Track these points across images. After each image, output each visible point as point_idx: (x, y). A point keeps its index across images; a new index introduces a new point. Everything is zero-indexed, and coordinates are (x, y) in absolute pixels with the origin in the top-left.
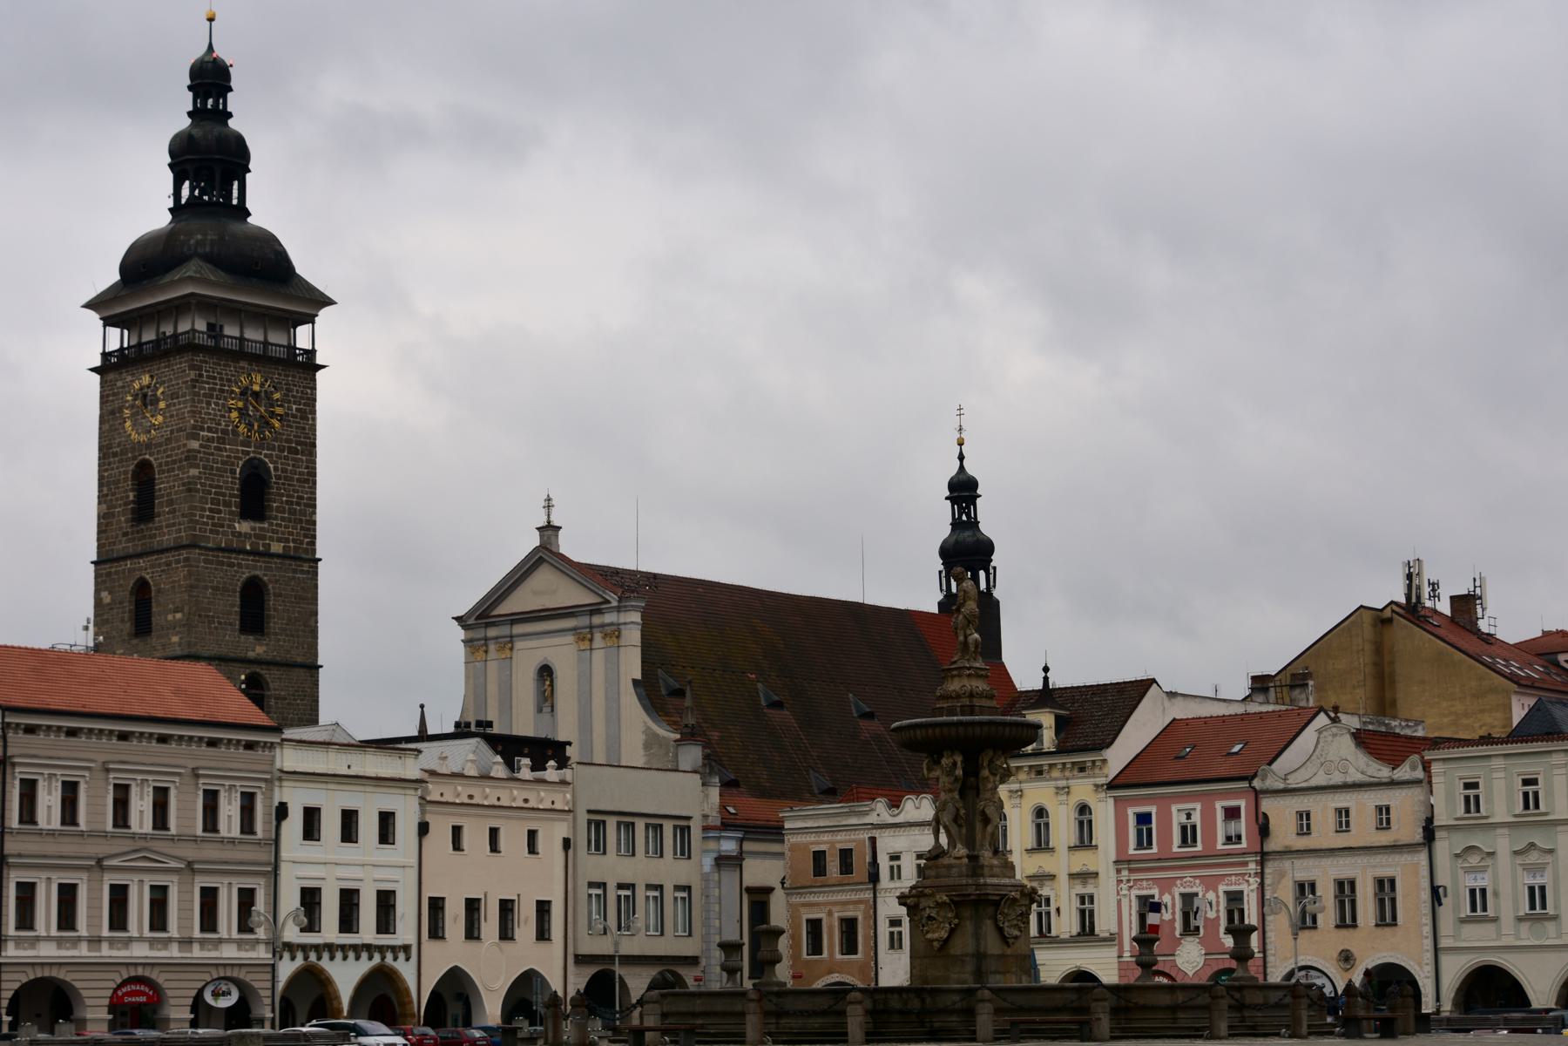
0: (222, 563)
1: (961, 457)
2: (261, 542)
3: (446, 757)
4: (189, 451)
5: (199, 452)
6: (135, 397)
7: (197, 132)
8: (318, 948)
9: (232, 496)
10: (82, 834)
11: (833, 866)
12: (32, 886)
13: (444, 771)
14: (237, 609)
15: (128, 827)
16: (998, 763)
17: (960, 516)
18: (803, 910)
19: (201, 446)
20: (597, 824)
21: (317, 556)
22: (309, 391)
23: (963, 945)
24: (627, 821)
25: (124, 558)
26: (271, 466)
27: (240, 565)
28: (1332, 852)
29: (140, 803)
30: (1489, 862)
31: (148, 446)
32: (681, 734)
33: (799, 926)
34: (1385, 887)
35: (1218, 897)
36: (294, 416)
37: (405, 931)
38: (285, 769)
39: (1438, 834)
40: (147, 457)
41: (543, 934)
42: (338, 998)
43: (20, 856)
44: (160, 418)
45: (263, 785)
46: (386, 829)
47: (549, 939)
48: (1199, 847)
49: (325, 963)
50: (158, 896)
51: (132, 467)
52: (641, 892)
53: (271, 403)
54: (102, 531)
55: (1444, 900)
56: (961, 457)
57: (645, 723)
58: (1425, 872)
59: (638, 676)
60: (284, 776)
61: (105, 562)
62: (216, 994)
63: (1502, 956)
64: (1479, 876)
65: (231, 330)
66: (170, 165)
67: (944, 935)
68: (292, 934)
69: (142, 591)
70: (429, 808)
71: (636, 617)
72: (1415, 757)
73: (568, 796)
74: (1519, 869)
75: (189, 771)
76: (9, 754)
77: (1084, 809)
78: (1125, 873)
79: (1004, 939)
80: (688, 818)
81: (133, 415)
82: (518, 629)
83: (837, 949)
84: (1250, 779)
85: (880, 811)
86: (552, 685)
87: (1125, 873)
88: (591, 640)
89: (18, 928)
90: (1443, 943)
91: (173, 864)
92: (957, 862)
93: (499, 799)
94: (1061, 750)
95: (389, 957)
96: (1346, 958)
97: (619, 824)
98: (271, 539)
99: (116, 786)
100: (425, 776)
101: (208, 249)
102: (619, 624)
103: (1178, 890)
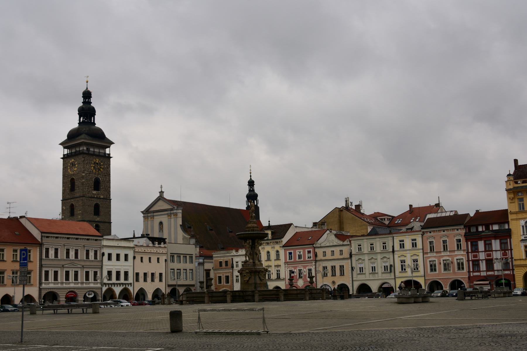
0: (90, 200)
1: (251, 176)
2: (98, 196)
3: (139, 242)
4: (82, 176)
5: (85, 176)
6: (71, 164)
8: (111, 284)
9: (92, 185)
10: (59, 260)
11: (224, 265)
12: (48, 271)
13: (139, 245)
14: (93, 210)
15: (69, 258)
16: (259, 242)
17: (251, 189)
18: (217, 274)
19: (85, 175)
20: (172, 256)
21: (111, 198)
22: (109, 163)
23: (252, 281)
24: (179, 255)
25: (68, 199)
26: (101, 179)
27: (94, 201)
28: (330, 260)
29: (72, 253)
30: (363, 262)
31: (73, 175)
32: (191, 236)
33: (217, 278)
34: (342, 267)
35: (306, 270)
36: (106, 168)
37: (131, 280)
38: (104, 245)
39: (353, 256)
40: (73, 177)
41: (161, 280)
42: (116, 295)
43: (45, 265)
44: (76, 169)
45: (99, 248)
46: (126, 258)
47: (162, 281)
48: (302, 259)
49: (113, 287)
50: (76, 273)
51: (70, 179)
52: (182, 271)
53: (101, 165)
54: (63, 193)
55: (354, 270)
56: (251, 176)
57: (183, 234)
58: (350, 264)
59: (181, 224)
60: (104, 246)
61: (64, 200)
62: (89, 294)
63: (367, 282)
64: (361, 265)
65: (92, 149)
66: (78, 114)
67: (248, 279)
68: (105, 281)
69: (72, 207)
70: (135, 253)
71: (181, 211)
72: (348, 240)
73: (166, 250)
74: (370, 263)
75: (82, 246)
76: (43, 242)
77: (277, 251)
78: (286, 265)
79: (261, 280)
80: (192, 255)
81: (70, 168)
82: (155, 214)
83: (225, 282)
84: (313, 244)
85: (234, 253)
86: (162, 226)
87: (286, 265)
88: (171, 216)
89: (45, 281)
90: (354, 279)
91: (79, 266)
92: (250, 263)
93: (151, 251)
94: (273, 239)
95: (127, 286)
96: (334, 282)
97: (177, 256)
98: (101, 195)
99: (66, 249)
100: (135, 246)
101: (86, 132)
102: (177, 213)
103: (298, 269)
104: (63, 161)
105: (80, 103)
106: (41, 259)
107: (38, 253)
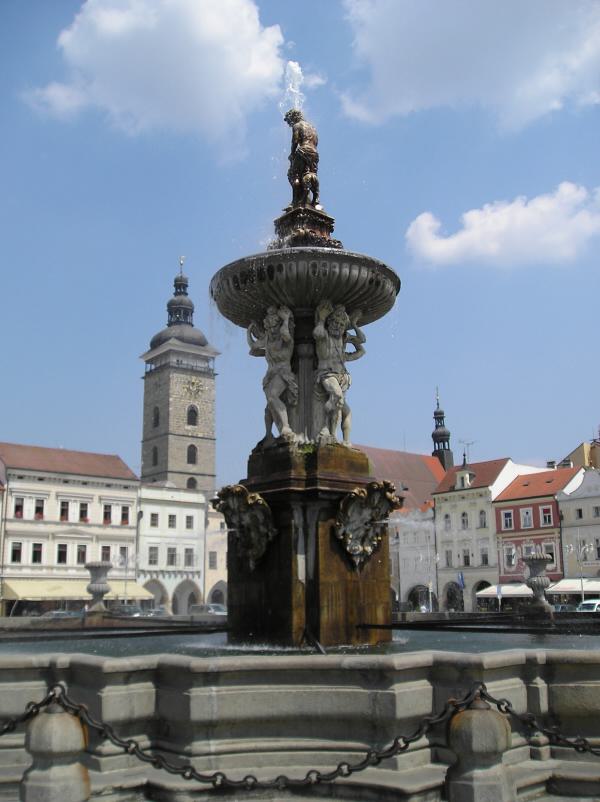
7: (176, 299)
8: (156, 572)
37: (199, 564)
49: (160, 578)
54: (144, 431)
61: (145, 440)
65: (185, 362)
68: (144, 565)
95: (190, 576)
104: (145, 383)
105: (169, 293)
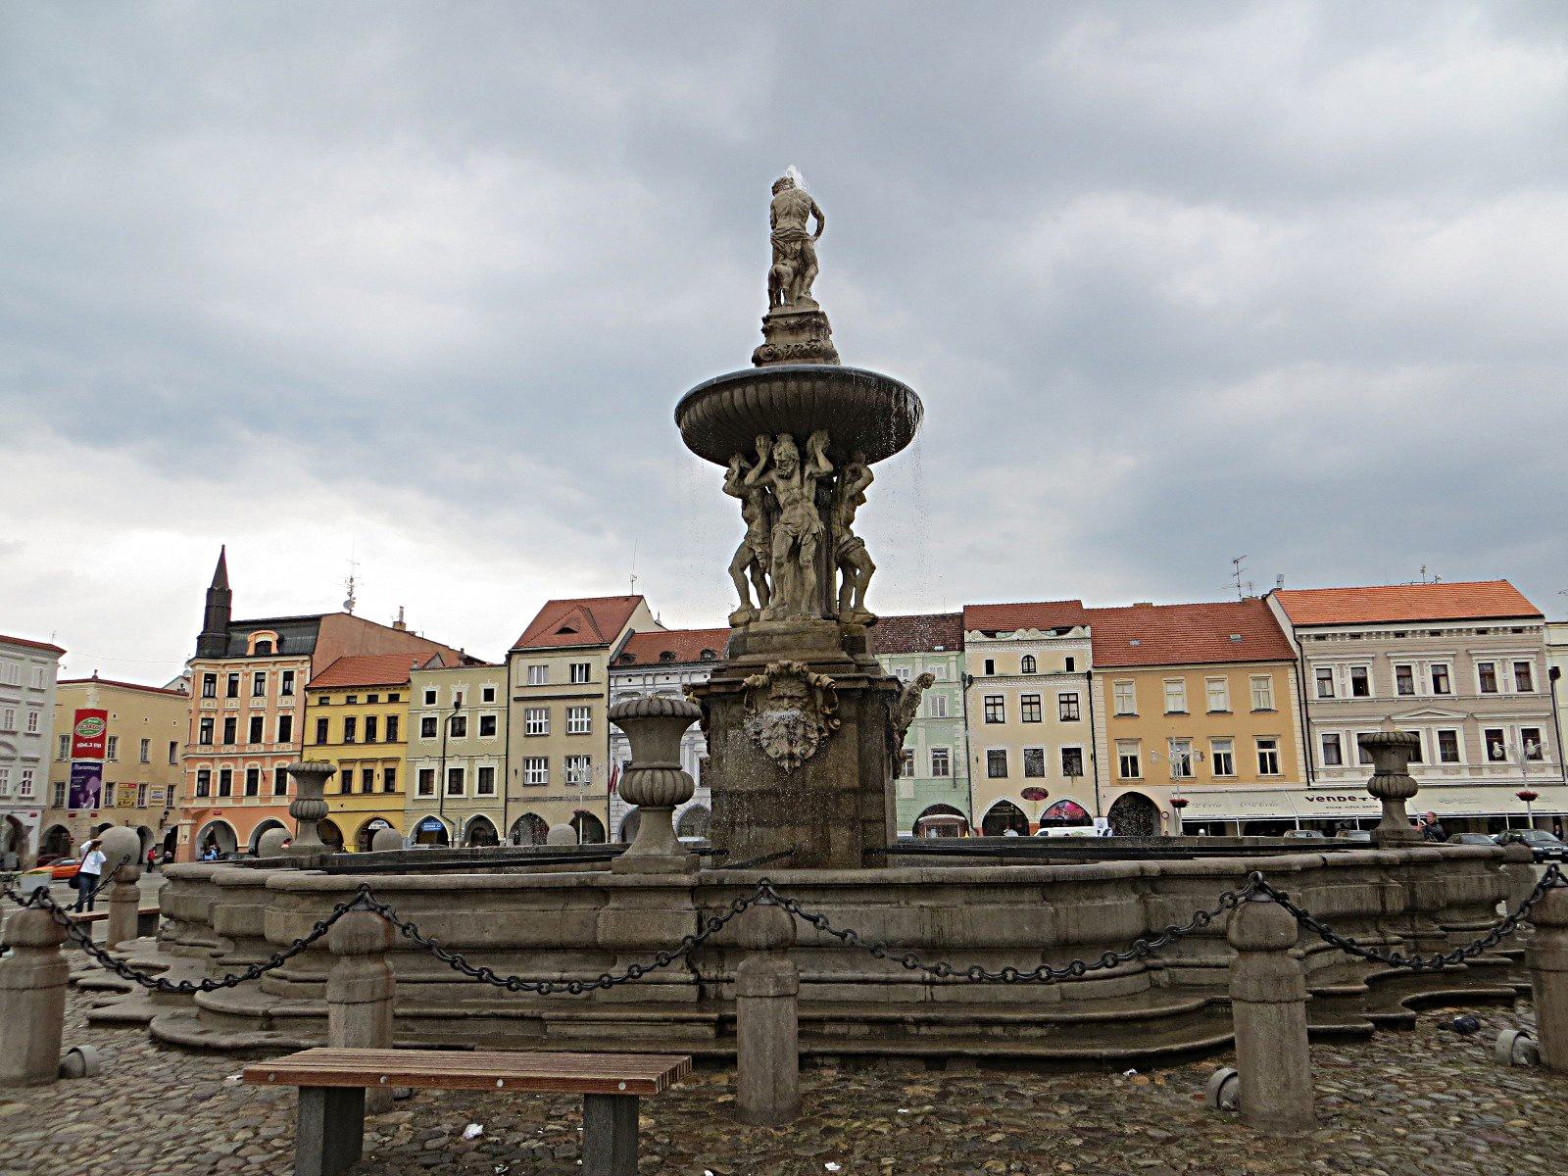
45: (1534, 656)
60: (1552, 649)
106: (1304, 703)
107: (1293, 687)
